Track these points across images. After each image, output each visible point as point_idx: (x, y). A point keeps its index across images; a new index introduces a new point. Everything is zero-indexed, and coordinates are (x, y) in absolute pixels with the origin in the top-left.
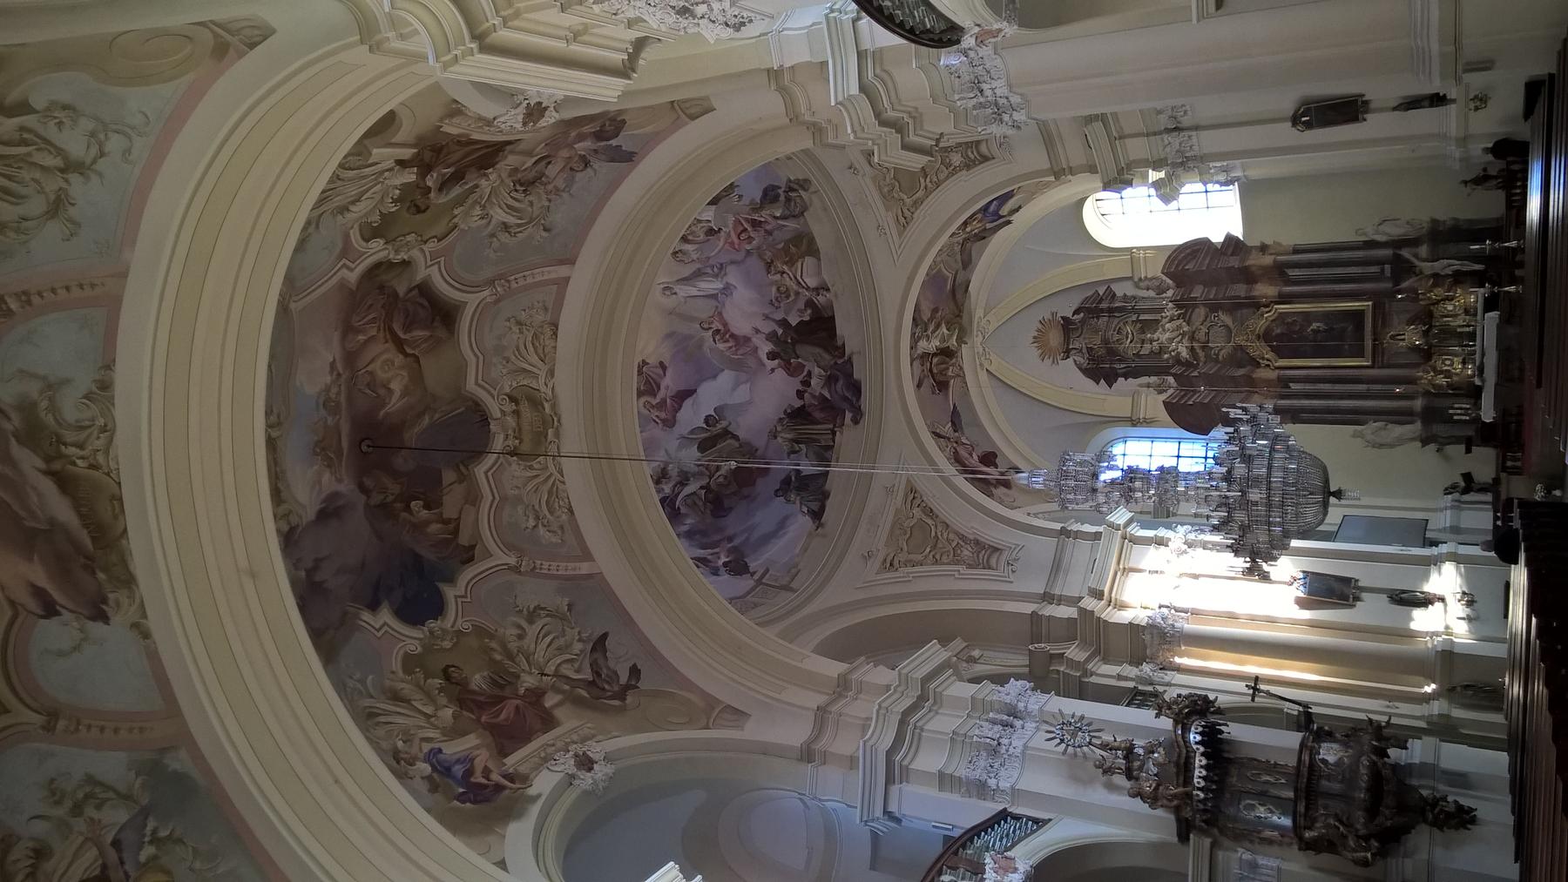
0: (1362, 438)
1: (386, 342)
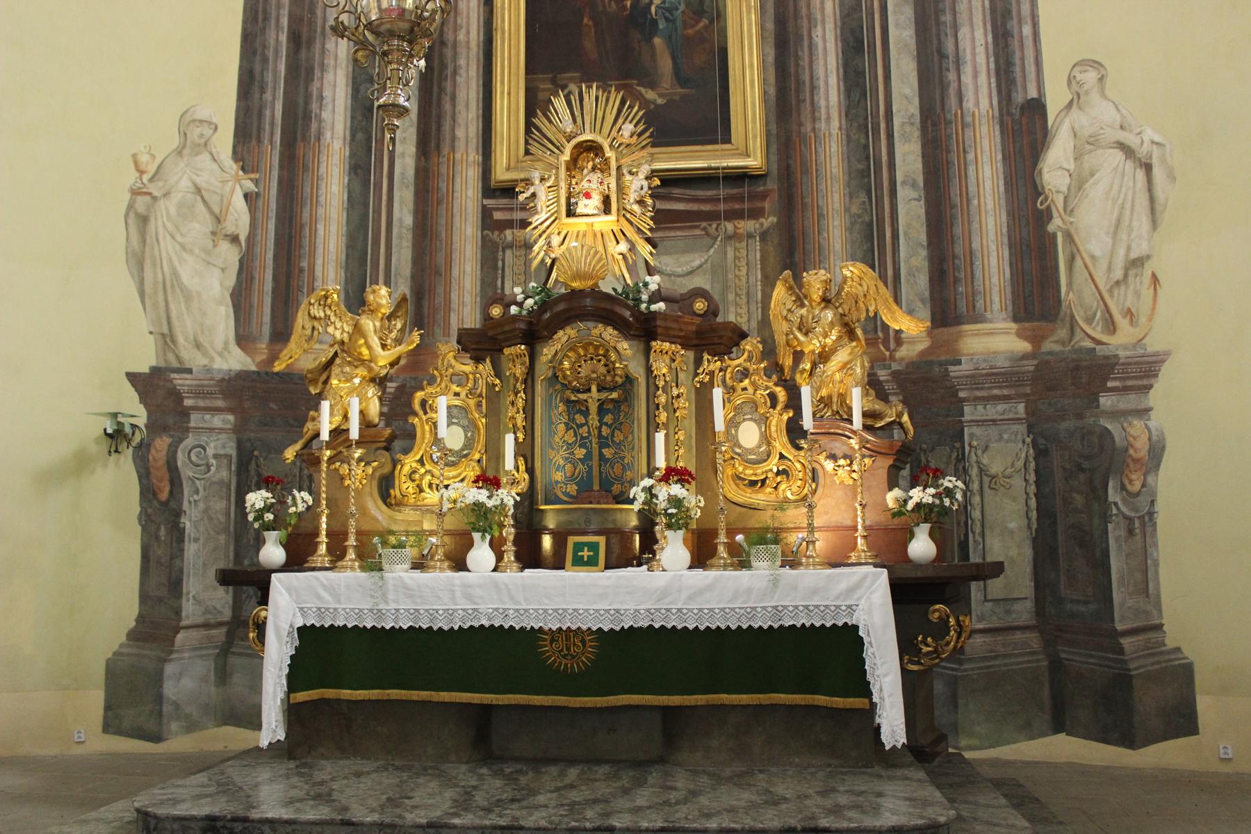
0: (179, 152)
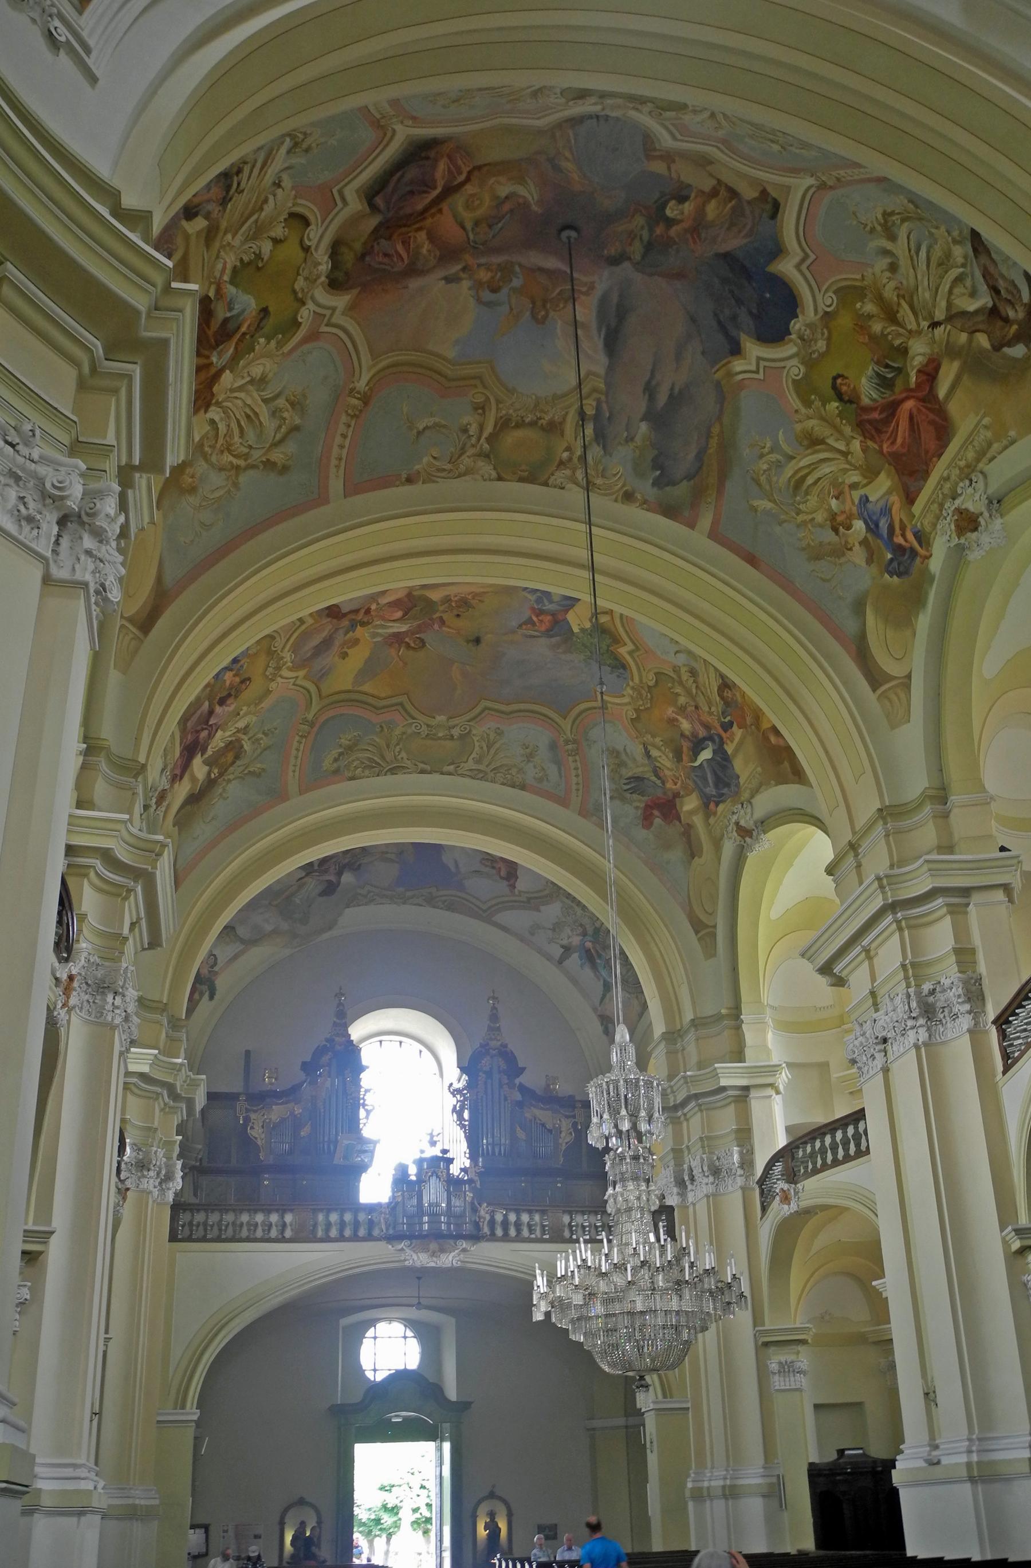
1: (440, 211)
